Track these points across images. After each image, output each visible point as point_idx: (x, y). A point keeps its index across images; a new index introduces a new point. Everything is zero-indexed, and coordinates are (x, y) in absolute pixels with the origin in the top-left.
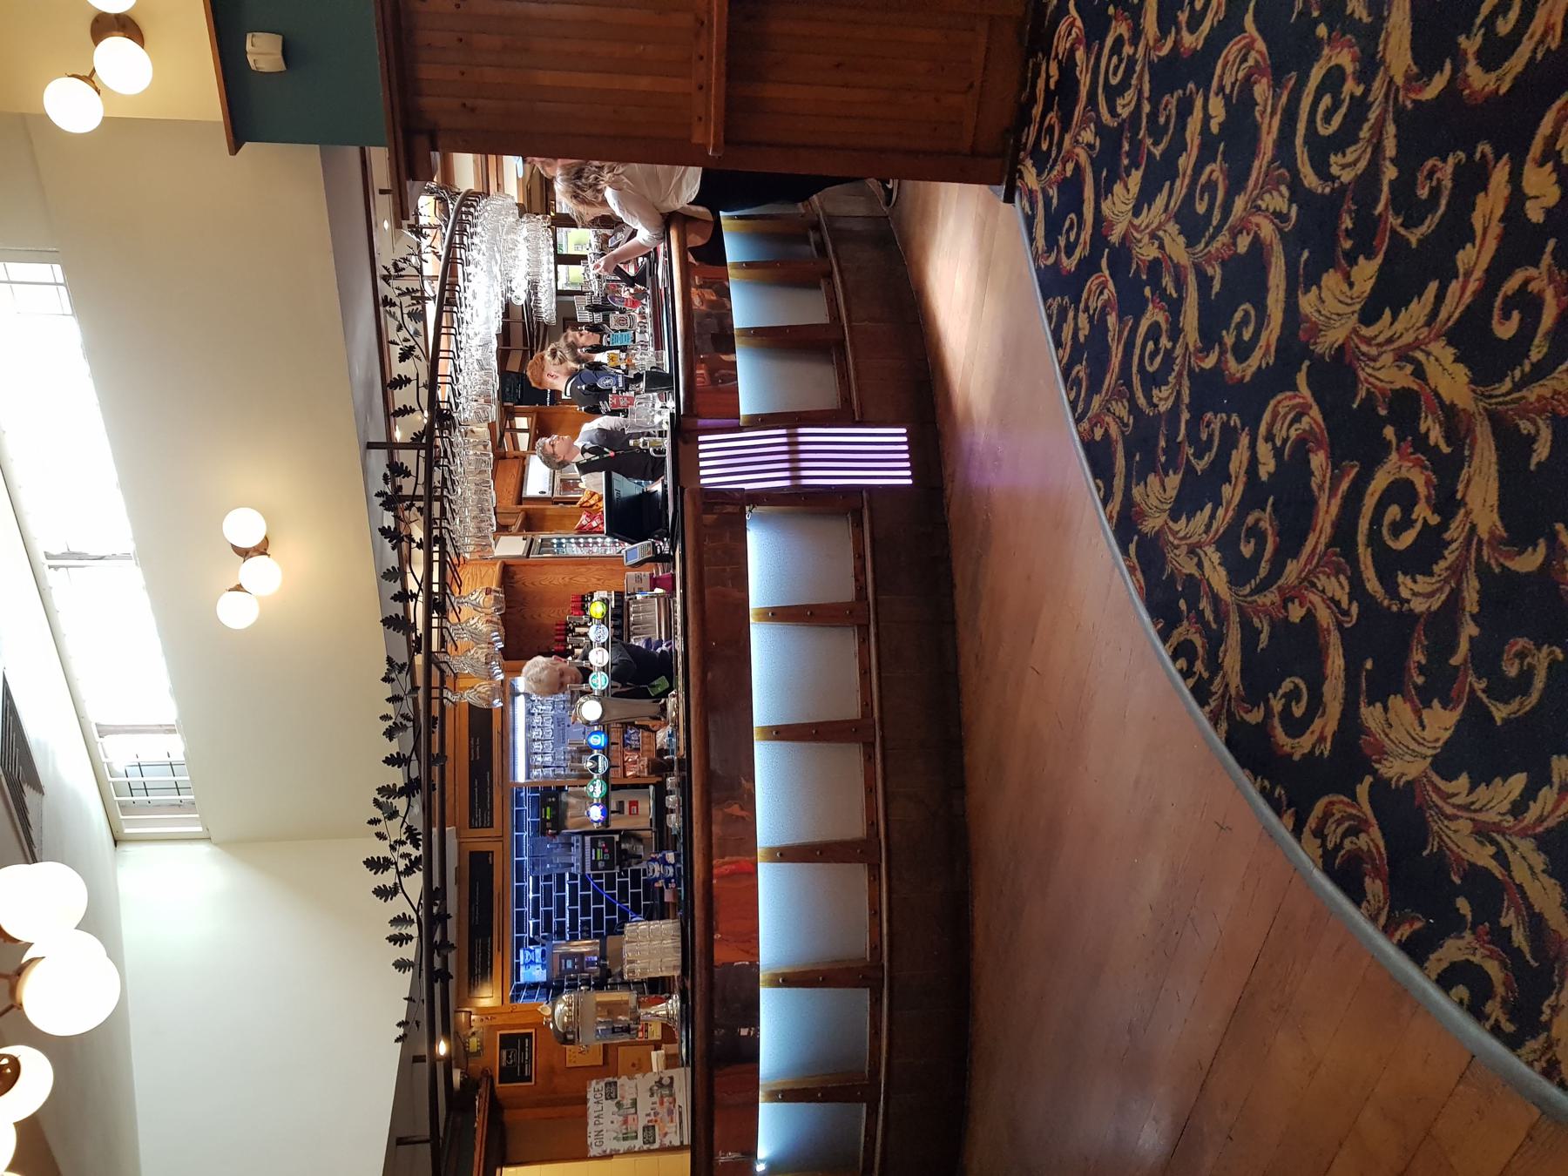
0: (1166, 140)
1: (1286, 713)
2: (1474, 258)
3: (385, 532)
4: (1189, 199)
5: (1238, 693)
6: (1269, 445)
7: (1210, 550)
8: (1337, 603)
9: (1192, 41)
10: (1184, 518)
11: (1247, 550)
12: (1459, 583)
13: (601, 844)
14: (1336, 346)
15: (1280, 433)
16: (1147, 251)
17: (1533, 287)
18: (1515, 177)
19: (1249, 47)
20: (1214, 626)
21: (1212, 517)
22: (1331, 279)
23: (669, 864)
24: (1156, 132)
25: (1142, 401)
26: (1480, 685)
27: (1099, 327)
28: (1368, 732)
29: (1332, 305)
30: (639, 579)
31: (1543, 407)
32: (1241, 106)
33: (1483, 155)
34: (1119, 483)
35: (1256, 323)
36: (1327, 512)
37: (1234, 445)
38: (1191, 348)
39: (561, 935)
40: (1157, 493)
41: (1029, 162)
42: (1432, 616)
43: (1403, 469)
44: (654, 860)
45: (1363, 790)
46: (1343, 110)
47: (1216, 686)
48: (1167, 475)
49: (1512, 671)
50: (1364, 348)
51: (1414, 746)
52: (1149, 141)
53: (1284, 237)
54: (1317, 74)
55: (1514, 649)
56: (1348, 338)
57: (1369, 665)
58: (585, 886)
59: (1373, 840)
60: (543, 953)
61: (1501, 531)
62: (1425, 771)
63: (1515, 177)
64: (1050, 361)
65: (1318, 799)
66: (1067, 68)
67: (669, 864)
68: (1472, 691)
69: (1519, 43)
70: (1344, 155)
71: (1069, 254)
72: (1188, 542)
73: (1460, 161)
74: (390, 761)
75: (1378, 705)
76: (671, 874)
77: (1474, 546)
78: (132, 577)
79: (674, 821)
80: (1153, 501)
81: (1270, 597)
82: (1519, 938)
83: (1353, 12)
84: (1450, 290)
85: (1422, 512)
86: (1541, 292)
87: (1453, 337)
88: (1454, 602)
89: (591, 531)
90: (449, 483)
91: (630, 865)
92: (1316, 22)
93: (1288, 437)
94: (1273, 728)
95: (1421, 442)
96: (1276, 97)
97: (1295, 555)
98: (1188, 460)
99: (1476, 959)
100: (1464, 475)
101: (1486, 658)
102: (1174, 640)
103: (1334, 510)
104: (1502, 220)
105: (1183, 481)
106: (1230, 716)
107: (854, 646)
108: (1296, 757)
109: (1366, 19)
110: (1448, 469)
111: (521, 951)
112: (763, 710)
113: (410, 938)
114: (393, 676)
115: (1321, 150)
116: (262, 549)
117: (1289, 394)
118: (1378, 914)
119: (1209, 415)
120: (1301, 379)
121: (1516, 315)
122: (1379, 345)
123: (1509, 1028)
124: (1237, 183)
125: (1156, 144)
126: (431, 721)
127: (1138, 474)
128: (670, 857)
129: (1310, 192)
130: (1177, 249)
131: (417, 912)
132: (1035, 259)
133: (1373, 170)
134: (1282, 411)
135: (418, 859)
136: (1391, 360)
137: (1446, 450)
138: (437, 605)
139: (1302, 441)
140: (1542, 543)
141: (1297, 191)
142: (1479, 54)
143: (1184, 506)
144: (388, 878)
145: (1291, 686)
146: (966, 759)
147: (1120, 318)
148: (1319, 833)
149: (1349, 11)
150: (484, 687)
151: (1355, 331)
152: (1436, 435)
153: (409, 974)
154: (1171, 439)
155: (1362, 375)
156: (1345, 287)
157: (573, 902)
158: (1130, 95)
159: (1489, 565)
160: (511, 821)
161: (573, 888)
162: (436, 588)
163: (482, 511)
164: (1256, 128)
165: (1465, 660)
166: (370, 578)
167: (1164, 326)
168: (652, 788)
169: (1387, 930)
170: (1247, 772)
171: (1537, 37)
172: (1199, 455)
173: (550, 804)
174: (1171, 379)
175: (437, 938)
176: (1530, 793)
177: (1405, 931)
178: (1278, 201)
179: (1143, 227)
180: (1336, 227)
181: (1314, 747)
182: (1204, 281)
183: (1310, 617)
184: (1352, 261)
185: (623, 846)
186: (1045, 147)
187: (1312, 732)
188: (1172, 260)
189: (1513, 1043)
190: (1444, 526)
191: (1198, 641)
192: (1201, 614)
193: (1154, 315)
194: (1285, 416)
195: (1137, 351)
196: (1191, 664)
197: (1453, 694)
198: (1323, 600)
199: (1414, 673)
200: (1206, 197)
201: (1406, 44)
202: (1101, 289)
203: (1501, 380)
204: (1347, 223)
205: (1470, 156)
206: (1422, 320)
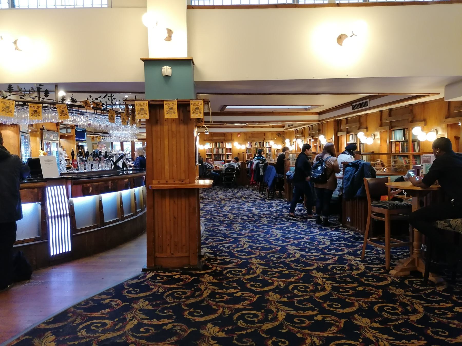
2: (155, 322)
15: (113, 303)
18: (170, 323)
19: (189, 279)
42: (78, 336)
46: (179, 296)
53: (154, 293)
61: (100, 341)
63: (170, 323)
103: (97, 315)
115: (172, 295)
121: (145, 330)
129: (164, 295)
133: (169, 303)
141: (163, 293)
182: (143, 282)
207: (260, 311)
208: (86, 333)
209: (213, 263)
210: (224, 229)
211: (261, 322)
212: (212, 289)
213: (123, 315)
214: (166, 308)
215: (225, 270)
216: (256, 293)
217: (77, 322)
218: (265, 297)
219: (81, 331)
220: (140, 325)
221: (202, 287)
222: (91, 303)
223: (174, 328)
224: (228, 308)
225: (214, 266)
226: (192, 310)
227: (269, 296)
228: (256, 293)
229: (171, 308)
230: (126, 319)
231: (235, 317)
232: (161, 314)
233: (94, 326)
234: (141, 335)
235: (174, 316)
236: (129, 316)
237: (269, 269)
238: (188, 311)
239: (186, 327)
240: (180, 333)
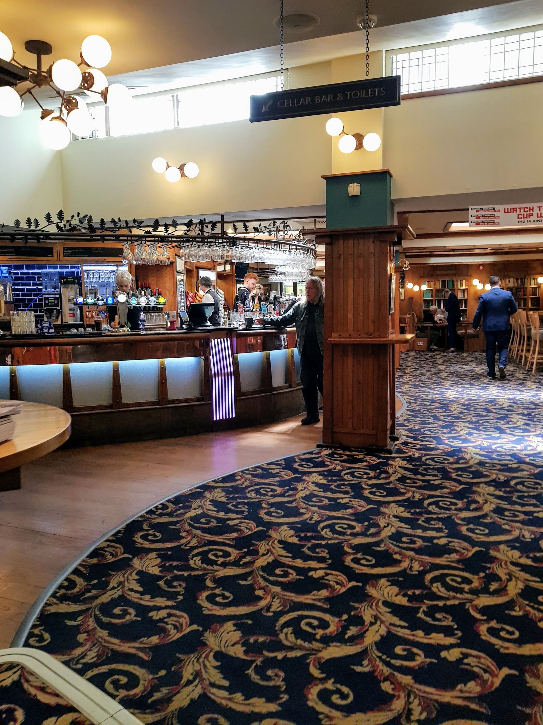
0: (336, 489)
2: (299, 563)
4: (316, 496)
7: (201, 511)
11: (203, 520)
13: (56, 302)
15: (242, 525)
16: (300, 486)
20: (175, 514)
22: (292, 532)
23: (49, 330)
24: (338, 486)
25: (250, 489)
26: (169, 578)
27: (274, 475)
29: (283, 534)
30: (173, 316)
31: (255, 582)
32: (346, 506)
39: (14, 284)
40: (219, 496)
41: (330, 452)
42: (189, 565)
44: (50, 324)
45: (127, 555)
47: (153, 516)
50: (271, 542)
51: (145, 565)
52: (336, 484)
60: (6, 277)
61: (217, 577)
64: (263, 462)
66: (361, 460)
67: (49, 330)
68: (166, 576)
76: (45, 331)
79: (74, 331)
80: (216, 495)
81: (187, 527)
88: (193, 569)
89: (187, 297)
90: (209, 244)
91: (46, 314)
99: (78, 586)
101: (177, 578)
102: (167, 504)
107: (150, 400)
108: (134, 539)
110: (236, 563)
111: (7, 268)
112: (124, 364)
114: (136, 223)
115: (332, 527)
119: (247, 507)
120: (261, 528)
123: (58, 595)
125: (335, 486)
127: (224, 489)
128: (52, 331)
131: (40, 230)
132: (297, 456)
134: (250, 525)
137: (241, 563)
138: (163, 239)
140: (215, 586)
141: (318, 522)
143: (215, 503)
144: (55, 219)
147: (278, 481)
148: (108, 546)
150: (130, 256)
154: (238, 498)
156: (289, 536)
158: (351, 478)
160: (64, 264)
161: (34, 290)
163: (199, 257)
164: (339, 511)
167: (275, 493)
168: (82, 323)
169: (80, 565)
172: (233, 505)
173: (74, 281)
176: (136, 592)
177: (82, 569)
178: (316, 518)
180: (307, 532)
182: (291, 502)
183: (183, 538)
185: (55, 311)
186: (335, 456)
189: (54, 595)
191: (169, 510)
192: (179, 510)
193: (279, 490)
195: (267, 486)
196: (160, 509)
199: (170, 563)
201: (360, 542)
202: (287, 475)
207: (477, 574)
208: (200, 561)
209: (410, 487)
210: (439, 430)
211: (475, 592)
212: (399, 527)
213: (254, 545)
214: (319, 546)
215: (427, 498)
216: (473, 543)
217: (191, 545)
218: (491, 551)
219: (195, 559)
220: (276, 564)
221: (382, 523)
222: (213, 522)
223: (326, 578)
224: (419, 561)
225: (409, 491)
226: (359, 556)
227: (498, 551)
228: (473, 543)
229: (327, 546)
230: (259, 553)
231: (429, 577)
232: (310, 553)
233: (213, 555)
234: (275, 578)
235: (329, 559)
236: (262, 547)
237: (508, 507)
238: (352, 557)
239: (344, 579)
240: (334, 587)
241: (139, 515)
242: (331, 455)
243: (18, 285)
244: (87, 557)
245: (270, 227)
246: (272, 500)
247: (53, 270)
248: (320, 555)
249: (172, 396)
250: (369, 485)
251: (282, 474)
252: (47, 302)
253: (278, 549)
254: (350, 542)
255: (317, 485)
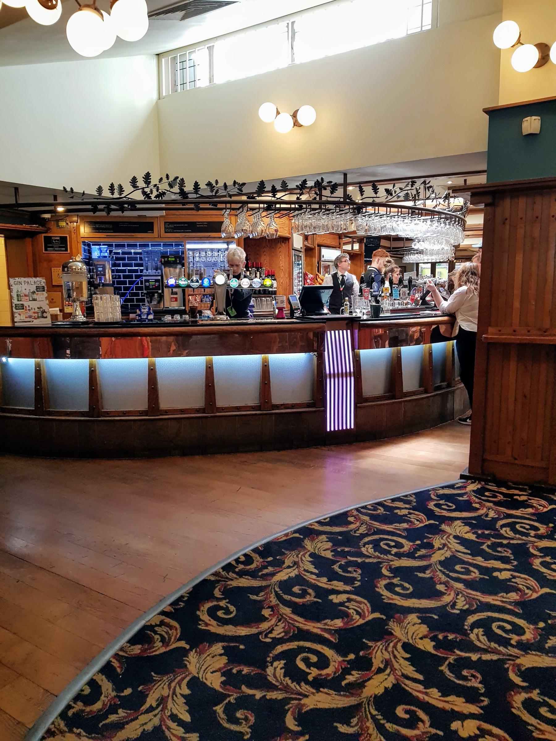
0: (490, 551)
1: (219, 608)
3: (305, 182)
4: (462, 562)
5: (228, 585)
6: (345, 600)
7: (296, 572)
8: (271, 632)
9: (537, 563)
10: (312, 559)
11: (296, 589)
12: (281, 690)
13: (157, 284)
14: (393, 631)
15: (351, 605)
16: (437, 542)
17: (420, 725)
18: (472, 716)
19: (534, 590)
20: (260, 574)
21: (312, 573)
22: (424, 629)
23: (147, 316)
24: (493, 546)
25: (366, 539)
26: (232, 699)
27: (401, 519)
28: (210, 647)
29: (412, 629)
30: (282, 302)
31: (364, 729)
33: (483, 701)
34: (328, 529)
35: (403, 594)
36: (314, 627)
37: (346, 583)
38: (391, 563)
39: (114, 265)
41: (479, 486)
42: (265, 677)
43: (334, 663)
44: (149, 309)
48: (332, 551)
49: (239, 715)
50: (391, 645)
51: (203, 668)
52: (489, 543)
53: (445, 606)
54: (521, 622)
55: (249, 716)
56: (396, 637)
57: (242, 647)
58: (137, 277)
59: (159, 649)
60: (105, 257)
61: (305, 710)
62: (191, 673)
63: (472, 716)
64: (385, 496)
65: (178, 623)
66: (524, 505)
67: (147, 316)
68: (229, 696)
69: (536, 718)
70: (483, 635)
71: (436, 505)
72: (300, 562)
73: (480, 690)
74: (196, 185)
75: (223, 651)
76: (143, 317)
77: (298, 697)
78: (283, 62)
79: (168, 318)
80: (319, 545)
81: (274, 600)
82: (113, 718)
83: (550, 639)
84: (419, 685)
85: (314, 672)
86: (418, 728)
87: (397, 687)
88: (271, 687)
89: (305, 279)
90: (328, 212)
91: (147, 298)
92: (546, 622)
93: (349, 609)
94: (212, 602)
95: (347, 671)
96: (510, 603)
97: (294, 612)
98: (338, 562)
99: (102, 698)
100: (331, 692)
103: (315, 631)
104: (452, 710)
105: (328, 559)
106: (218, 581)
107: (251, 403)
108: (198, 613)
109: (547, 646)
111: (106, 246)
113: (113, 194)
114: (237, 186)
115: (485, 624)
116: (296, 124)
117: (370, 609)
118: (124, 651)
119: (360, 571)
120: (377, 615)
121: (407, 716)
122: (393, 652)
123: (70, 713)
124: (470, 584)
125: (488, 546)
126: (215, 204)
127: (332, 538)
128: (151, 317)
129: (465, 619)
130: (438, 556)
131: (125, 197)
132: (433, 489)
134: (362, 606)
135: (150, 198)
136: (386, 657)
137: (343, 683)
138: (270, 206)
139: (347, 615)
140: (299, 729)
142: (530, 699)
143: (317, 559)
144: (141, 183)
145: (232, 610)
146: (197, 457)
147: (406, 529)
148: (162, 623)
149: (551, 637)
150: (231, 229)
151: (400, 640)
152: (350, 679)
153: (96, 193)
154: (349, 553)
155: (379, 644)
156: (420, 636)
157: (130, 271)
158: (511, 534)
159: (289, 704)
160: (168, 241)
161: (136, 271)
162: (278, 206)
163: (315, 228)
164: (496, 594)
165: (244, 693)
166: (282, 174)
167: (402, 550)
168: (184, 308)
169: (116, 656)
170: (191, 589)
171: (539, 726)
172: (341, 567)
173: (176, 260)
174: (377, 554)
175: (113, 207)
176: (181, 723)
177: (116, 664)
178: (461, 604)
179: (449, 540)
180: (449, 631)
181: (203, 621)
182: (423, 569)
183: (264, 619)
184: (432, 639)
185: (156, 294)
186: (487, 494)
187: (210, 620)
188: (433, 554)
189: (63, 715)
190: (307, 682)
191: (253, 566)
192: (266, 567)
193: (407, 546)
194: (359, 607)
195: (390, 537)
196: (242, 563)
197: (228, 687)
198: (272, 625)
199: (238, 668)
200: (463, 570)
201: (535, 665)
203: (376, 709)
204: (451, 637)
205: (482, 695)
206: (405, 672)
241: (213, 571)
242: (480, 492)
243: (119, 265)
244: (129, 642)
245: (407, 188)
246: (397, 563)
247: (156, 249)
248: (469, 684)
249: (276, 400)
250: (541, 550)
251: (412, 518)
252: (147, 284)
253: (402, 661)
254: (518, 661)
255: (463, 541)
